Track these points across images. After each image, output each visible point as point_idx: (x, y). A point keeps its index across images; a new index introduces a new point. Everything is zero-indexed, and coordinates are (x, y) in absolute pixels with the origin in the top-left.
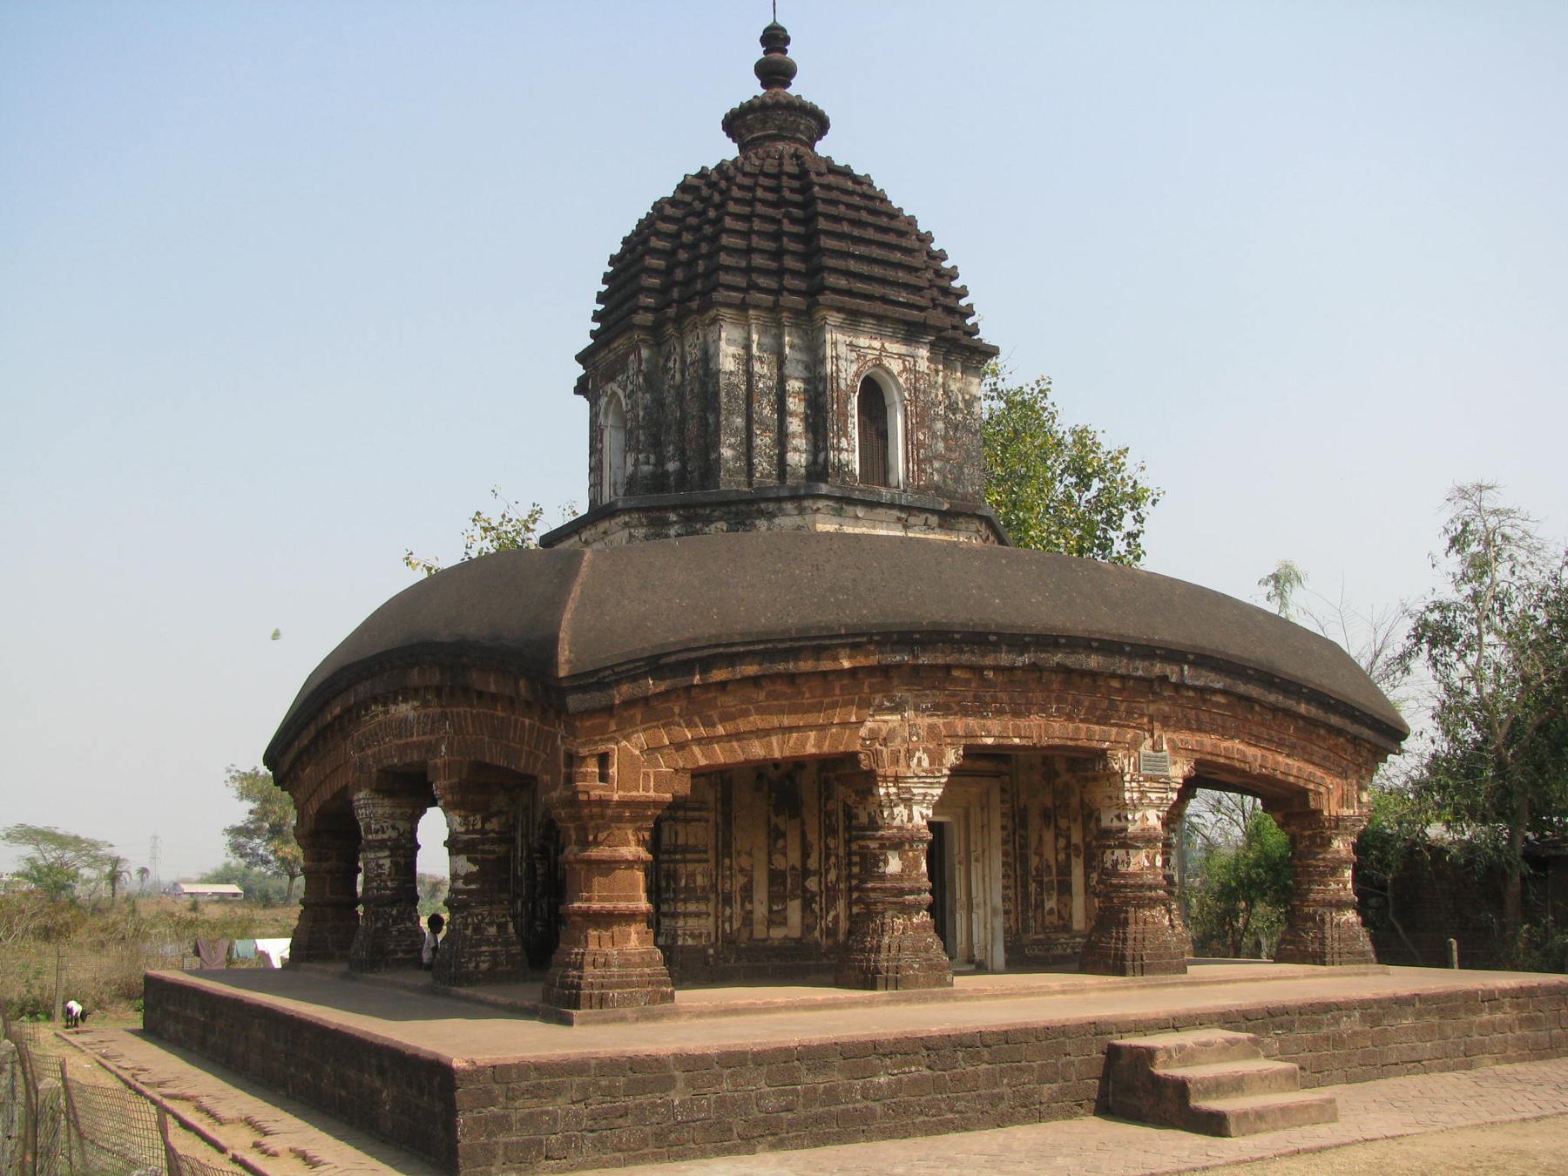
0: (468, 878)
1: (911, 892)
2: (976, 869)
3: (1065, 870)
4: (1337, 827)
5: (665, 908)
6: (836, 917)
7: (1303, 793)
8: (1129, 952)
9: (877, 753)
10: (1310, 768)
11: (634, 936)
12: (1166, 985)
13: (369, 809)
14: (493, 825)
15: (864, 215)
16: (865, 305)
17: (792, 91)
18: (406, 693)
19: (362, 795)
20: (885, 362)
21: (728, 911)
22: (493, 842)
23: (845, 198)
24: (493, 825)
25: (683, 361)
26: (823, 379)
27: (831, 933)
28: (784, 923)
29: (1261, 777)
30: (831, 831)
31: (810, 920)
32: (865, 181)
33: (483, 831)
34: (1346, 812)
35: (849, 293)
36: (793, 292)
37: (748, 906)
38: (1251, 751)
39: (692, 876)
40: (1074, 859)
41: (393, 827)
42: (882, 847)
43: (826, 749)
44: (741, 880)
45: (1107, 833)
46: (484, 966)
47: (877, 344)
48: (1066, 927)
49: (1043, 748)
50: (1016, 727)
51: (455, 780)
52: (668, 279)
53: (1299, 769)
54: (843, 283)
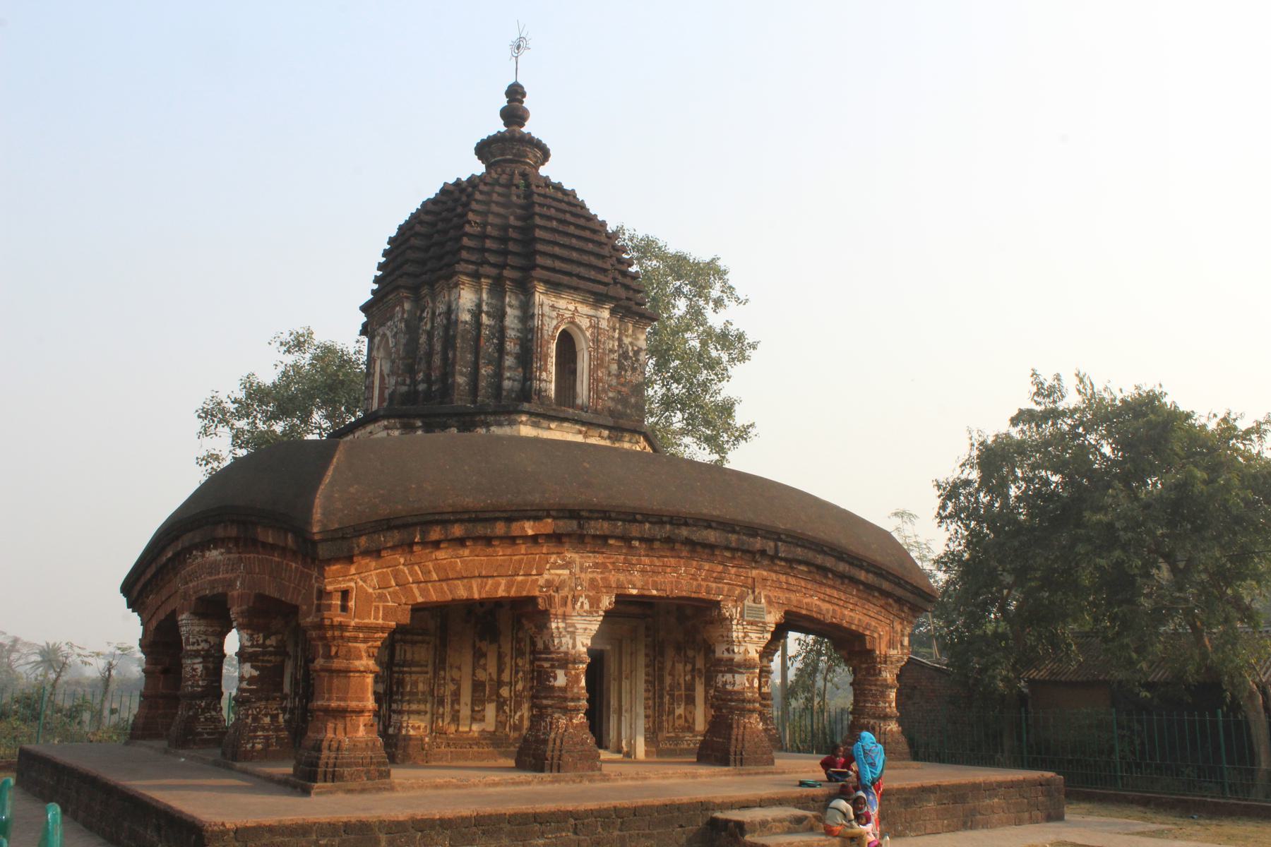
0: (251, 680)
1: (573, 700)
2: (626, 684)
3: (691, 688)
4: (885, 662)
5: (394, 706)
6: (521, 717)
7: (860, 637)
8: (732, 749)
9: (550, 598)
10: (866, 619)
11: (362, 728)
12: (757, 774)
13: (188, 626)
14: (272, 641)
15: (568, 217)
16: (565, 279)
17: (525, 130)
18: (216, 542)
19: (184, 616)
21: (441, 710)
22: (271, 654)
23: (555, 204)
24: (272, 641)
25: (433, 313)
26: (531, 330)
27: (516, 728)
28: (482, 720)
30: (521, 653)
31: (503, 718)
32: (572, 194)
33: (263, 646)
35: (553, 270)
36: (513, 267)
37: (457, 707)
38: (825, 606)
39: (415, 684)
40: (697, 679)
41: (206, 641)
42: (553, 666)
43: (513, 593)
44: (452, 687)
45: (720, 660)
46: (259, 746)
47: (571, 307)
48: (690, 728)
50: (655, 583)
51: (245, 607)
52: (428, 250)
54: (549, 262)
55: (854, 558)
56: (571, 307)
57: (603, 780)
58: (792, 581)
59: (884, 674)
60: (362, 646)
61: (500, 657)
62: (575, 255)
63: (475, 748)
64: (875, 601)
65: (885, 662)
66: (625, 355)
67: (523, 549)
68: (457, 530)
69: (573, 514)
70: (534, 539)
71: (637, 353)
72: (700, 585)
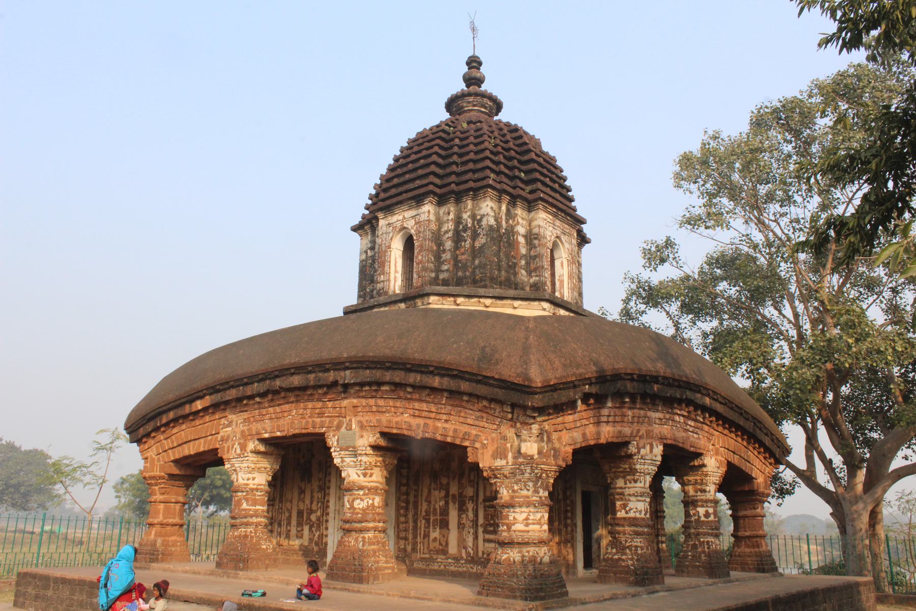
3: (445, 512)
11: (153, 533)
12: (334, 588)
16: (388, 202)
20: (405, 225)
28: (301, 537)
34: (499, 463)
35: (400, 194)
38: (414, 422)
40: (451, 505)
43: (206, 449)
44: (287, 515)
47: (401, 217)
48: (444, 552)
50: (278, 426)
53: (455, 431)
55: (420, 365)
56: (401, 217)
57: (234, 578)
58: (381, 402)
59: (501, 491)
60: (157, 488)
61: (312, 492)
62: (407, 176)
63: (295, 557)
64: (469, 406)
65: (496, 477)
67: (207, 418)
68: (171, 415)
69: (213, 390)
70: (205, 409)
71: (480, 221)
72: (307, 422)
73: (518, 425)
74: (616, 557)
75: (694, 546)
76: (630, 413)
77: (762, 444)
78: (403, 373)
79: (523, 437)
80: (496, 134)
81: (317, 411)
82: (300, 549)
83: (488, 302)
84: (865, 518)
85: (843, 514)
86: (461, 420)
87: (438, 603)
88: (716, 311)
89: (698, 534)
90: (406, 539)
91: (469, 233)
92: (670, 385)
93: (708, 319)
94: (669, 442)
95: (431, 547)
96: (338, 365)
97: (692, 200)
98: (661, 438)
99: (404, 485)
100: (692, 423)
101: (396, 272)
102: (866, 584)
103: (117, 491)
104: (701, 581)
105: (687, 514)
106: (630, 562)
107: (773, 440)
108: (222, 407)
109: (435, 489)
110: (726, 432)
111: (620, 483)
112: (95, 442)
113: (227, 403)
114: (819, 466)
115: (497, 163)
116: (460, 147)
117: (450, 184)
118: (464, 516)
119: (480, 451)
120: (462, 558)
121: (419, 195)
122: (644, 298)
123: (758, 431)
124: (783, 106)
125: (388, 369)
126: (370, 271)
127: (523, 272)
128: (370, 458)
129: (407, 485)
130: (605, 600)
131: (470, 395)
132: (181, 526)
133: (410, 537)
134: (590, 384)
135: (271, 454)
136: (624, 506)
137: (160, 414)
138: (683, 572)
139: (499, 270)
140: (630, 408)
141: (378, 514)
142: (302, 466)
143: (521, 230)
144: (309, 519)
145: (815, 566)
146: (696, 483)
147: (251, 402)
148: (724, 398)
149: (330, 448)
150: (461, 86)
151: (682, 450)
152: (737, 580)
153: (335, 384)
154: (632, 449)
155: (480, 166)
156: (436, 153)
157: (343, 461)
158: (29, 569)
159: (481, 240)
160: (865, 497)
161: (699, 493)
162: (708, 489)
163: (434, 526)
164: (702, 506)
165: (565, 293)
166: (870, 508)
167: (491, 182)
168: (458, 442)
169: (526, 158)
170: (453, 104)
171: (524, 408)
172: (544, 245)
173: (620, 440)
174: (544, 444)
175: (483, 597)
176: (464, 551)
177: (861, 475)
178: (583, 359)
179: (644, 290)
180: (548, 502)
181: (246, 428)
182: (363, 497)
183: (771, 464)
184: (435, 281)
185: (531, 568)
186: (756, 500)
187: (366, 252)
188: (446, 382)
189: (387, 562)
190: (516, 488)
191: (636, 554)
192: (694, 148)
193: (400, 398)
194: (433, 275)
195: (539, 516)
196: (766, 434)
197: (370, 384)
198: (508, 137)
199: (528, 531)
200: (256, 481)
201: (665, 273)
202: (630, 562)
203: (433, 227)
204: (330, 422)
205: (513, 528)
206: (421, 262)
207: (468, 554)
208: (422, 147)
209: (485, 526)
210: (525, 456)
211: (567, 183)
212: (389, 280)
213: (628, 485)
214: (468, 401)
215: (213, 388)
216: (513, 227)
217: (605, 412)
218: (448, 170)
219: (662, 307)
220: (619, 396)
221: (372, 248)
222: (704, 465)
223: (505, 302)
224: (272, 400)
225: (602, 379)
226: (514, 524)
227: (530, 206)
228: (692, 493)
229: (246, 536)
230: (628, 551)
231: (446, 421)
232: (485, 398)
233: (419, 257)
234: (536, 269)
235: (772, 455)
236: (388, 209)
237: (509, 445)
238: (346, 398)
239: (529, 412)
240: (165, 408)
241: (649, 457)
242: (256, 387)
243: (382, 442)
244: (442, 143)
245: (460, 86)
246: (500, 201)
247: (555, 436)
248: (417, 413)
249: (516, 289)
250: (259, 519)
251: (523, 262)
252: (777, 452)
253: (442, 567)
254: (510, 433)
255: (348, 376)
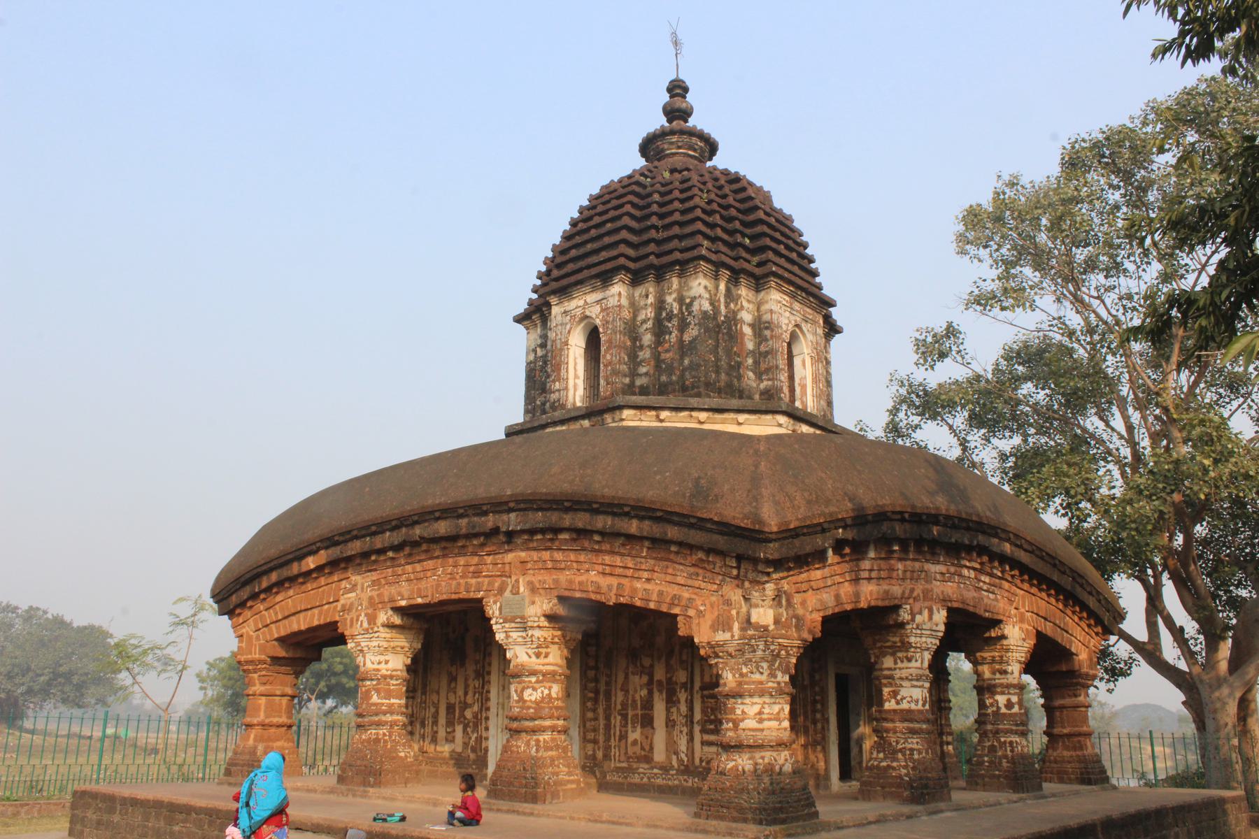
3: (648, 705)
10: (674, 590)
11: (252, 736)
12: (498, 810)
16: (565, 282)
20: (588, 313)
28: (453, 741)
29: (619, 606)
34: (721, 636)
35: (580, 270)
38: (604, 582)
43: (322, 622)
44: (433, 710)
48: (648, 759)
49: (436, 605)
50: (419, 589)
53: (661, 593)
55: (611, 505)
56: (581, 303)
57: (362, 797)
58: (558, 556)
59: (724, 675)
60: (256, 676)
61: (466, 680)
62: (589, 247)
63: (445, 768)
65: (717, 656)
66: (670, 317)
67: (323, 581)
68: (274, 577)
70: (320, 569)
72: (459, 584)
73: (747, 584)
74: (884, 764)
75: (992, 749)
76: (900, 566)
77: (1084, 607)
78: (587, 515)
79: (754, 601)
80: (710, 186)
81: (472, 569)
82: (451, 758)
83: (703, 416)
84: (1232, 708)
85: (1201, 703)
86: (669, 578)
87: (640, 830)
88: (1017, 423)
89: (997, 732)
90: (595, 742)
91: (675, 322)
92: (955, 527)
93: (1007, 434)
94: (955, 605)
95: (630, 752)
96: (500, 506)
97: (982, 270)
98: (944, 600)
99: (591, 668)
100: (987, 579)
101: (576, 377)
102: (1234, 800)
103: (202, 681)
104: (1003, 796)
105: (982, 705)
106: (904, 771)
107: (1099, 601)
108: (343, 565)
109: (633, 674)
110: (1034, 590)
111: (888, 662)
112: (171, 614)
113: (348, 560)
114: (1166, 637)
115: (712, 226)
116: (661, 205)
117: (647, 256)
118: (674, 710)
119: (695, 621)
120: (672, 767)
121: (606, 272)
122: (917, 408)
123: (1079, 589)
124: (1107, 139)
125: (567, 510)
126: (540, 376)
127: (751, 374)
128: (543, 633)
129: (596, 668)
130: (870, 823)
131: (680, 544)
132: (290, 727)
133: (601, 738)
134: (845, 527)
135: (410, 629)
136: (895, 694)
137: (258, 576)
138: (977, 784)
139: (717, 372)
140: (900, 559)
141: (557, 708)
142: (453, 643)
143: (747, 317)
144: (462, 715)
145: (1162, 776)
146: (993, 661)
147: (382, 558)
148: (1031, 544)
149: (490, 619)
150: (660, 121)
151: (974, 616)
152: (1054, 795)
153: (495, 531)
154: (904, 615)
155: (688, 230)
156: (628, 214)
157: (507, 637)
158: (87, 787)
159: (692, 332)
160: (1231, 679)
161: (998, 676)
162: (1010, 669)
163: (633, 723)
164: (1003, 693)
165: (809, 402)
166: (1238, 695)
167: (704, 252)
168: (664, 609)
169: (751, 217)
170: (650, 147)
171: (755, 561)
172: (779, 337)
173: (886, 603)
174: (783, 610)
175: (702, 821)
176: (674, 757)
177: (1225, 649)
178: (836, 494)
179: (918, 396)
180: (790, 689)
181: (375, 593)
182: (537, 685)
183: (1097, 634)
184: (630, 389)
185: (766, 780)
186: (1078, 684)
187: (535, 351)
188: (647, 527)
189: (570, 774)
190: (745, 670)
191: (911, 759)
192: (985, 199)
193: (583, 549)
194: (627, 380)
195: (776, 708)
196: (1090, 593)
197: (543, 531)
198: (727, 190)
199: (762, 730)
200: (390, 665)
201: (946, 373)
202: (904, 771)
203: (626, 314)
204: (489, 583)
205: (742, 725)
206: (610, 363)
207: (680, 761)
208: (609, 206)
209: (703, 723)
210: (757, 627)
211: (809, 251)
212: (566, 389)
213: (900, 665)
214: (677, 553)
215: (328, 539)
216: (735, 313)
217: (866, 564)
218: (645, 237)
219: (943, 419)
220: (885, 542)
221: (543, 346)
222: (1004, 637)
223: (726, 416)
224: (410, 555)
225: (861, 519)
226: (743, 720)
227: (759, 283)
228: (987, 675)
229: (377, 741)
230: (900, 756)
231: (648, 580)
232: (700, 548)
233: (606, 356)
234: (767, 370)
235: (1099, 621)
236: (564, 292)
237: (734, 612)
238: (510, 551)
239: (760, 567)
240: (264, 568)
241: (927, 626)
242: (388, 538)
243: (561, 610)
244: (636, 200)
245: (660, 121)
246: (716, 277)
247: (797, 599)
248: (608, 570)
249: (741, 397)
250: (395, 717)
251: (750, 361)
252: (1106, 618)
253: (645, 780)
254: (736, 595)
255: (512, 521)
